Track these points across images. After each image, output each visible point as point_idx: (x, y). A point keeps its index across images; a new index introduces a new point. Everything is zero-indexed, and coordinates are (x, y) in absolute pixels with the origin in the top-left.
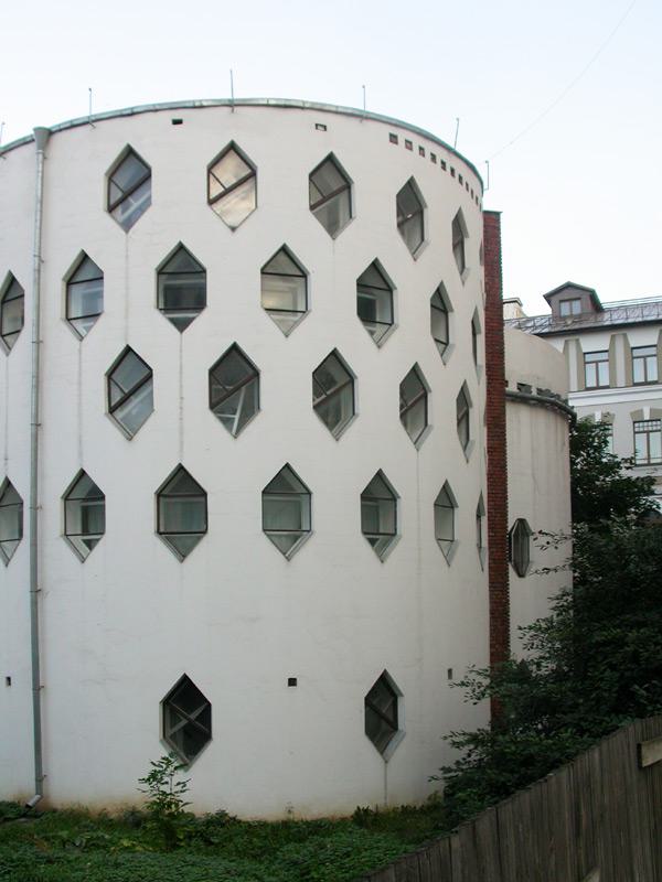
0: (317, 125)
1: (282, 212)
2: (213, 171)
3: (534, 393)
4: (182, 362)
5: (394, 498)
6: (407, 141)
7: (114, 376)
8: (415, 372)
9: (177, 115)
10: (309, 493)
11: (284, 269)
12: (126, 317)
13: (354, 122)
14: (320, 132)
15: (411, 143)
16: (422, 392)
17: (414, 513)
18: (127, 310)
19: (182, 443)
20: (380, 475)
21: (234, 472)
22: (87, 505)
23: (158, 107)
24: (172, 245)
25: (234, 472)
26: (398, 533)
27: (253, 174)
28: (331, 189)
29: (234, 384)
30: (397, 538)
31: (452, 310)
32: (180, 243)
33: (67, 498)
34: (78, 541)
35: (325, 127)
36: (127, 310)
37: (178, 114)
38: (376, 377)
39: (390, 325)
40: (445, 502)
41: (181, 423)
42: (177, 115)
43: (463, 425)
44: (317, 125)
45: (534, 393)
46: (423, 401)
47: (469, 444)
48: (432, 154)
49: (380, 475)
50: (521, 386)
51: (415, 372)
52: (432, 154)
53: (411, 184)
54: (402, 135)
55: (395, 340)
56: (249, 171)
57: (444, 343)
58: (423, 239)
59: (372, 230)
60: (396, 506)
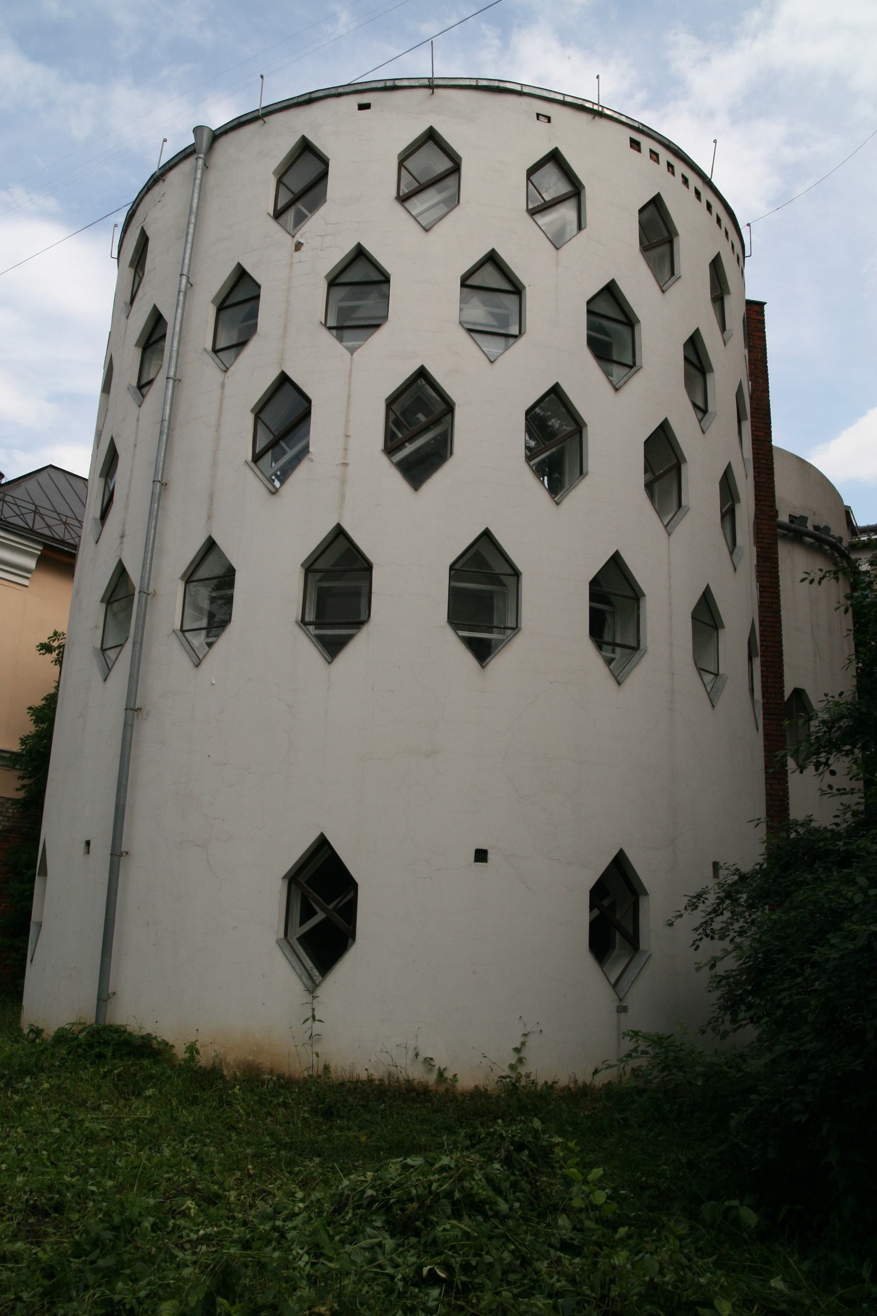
0: (538, 115)
1: (491, 211)
2: (405, 163)
3: (810, 528)
4: (351, 392)
5: (636, 595)
6: (651, 151)
7: (262, 416)
8: (664, 429)
9: (365, 99)
10: (517, 574)
11: (493, 282)
12: (284, 337)
13: (585, 117)
14: (542, 124)
15: (657, 155)
16: (675, 461)
17: (665, 619)
18: (285, 330)
19: (343, 496)
20: (616, 560)
21: (416, 543)
22: (214, 583)
23: (341, 90)
24: (347, 248)
25: (416, 543)
26: (642, 646)
27: (456, 169)
28: (557, 185)
29: (419, 426)
30: (638, 654)
31: (712, 370)
32: (359, 245)
33: (189, 578)
34: (198, 640)
35: (549, 119)
36: (285, 330)
37: (364, 94)
38: (615, 421)
39: (631, 367)
40: (706, 616)
41: (349, 475)
42: (365, 99)
43: (728, 518)
44: (538, 115)
45: (810, 528)
46: (674, 472)
47: (736, 549)
48: (683, 176)
49: (616, 560)
50: (792, 519)
51: (664, 429)
52: (683, 176)
53: (657, 202)
54: (647, 144)
55: (637, 383)
56: (448, 164)
57: (702, 410)
58: (673, 274)
59: (609, 249)
60: (638, 608)
